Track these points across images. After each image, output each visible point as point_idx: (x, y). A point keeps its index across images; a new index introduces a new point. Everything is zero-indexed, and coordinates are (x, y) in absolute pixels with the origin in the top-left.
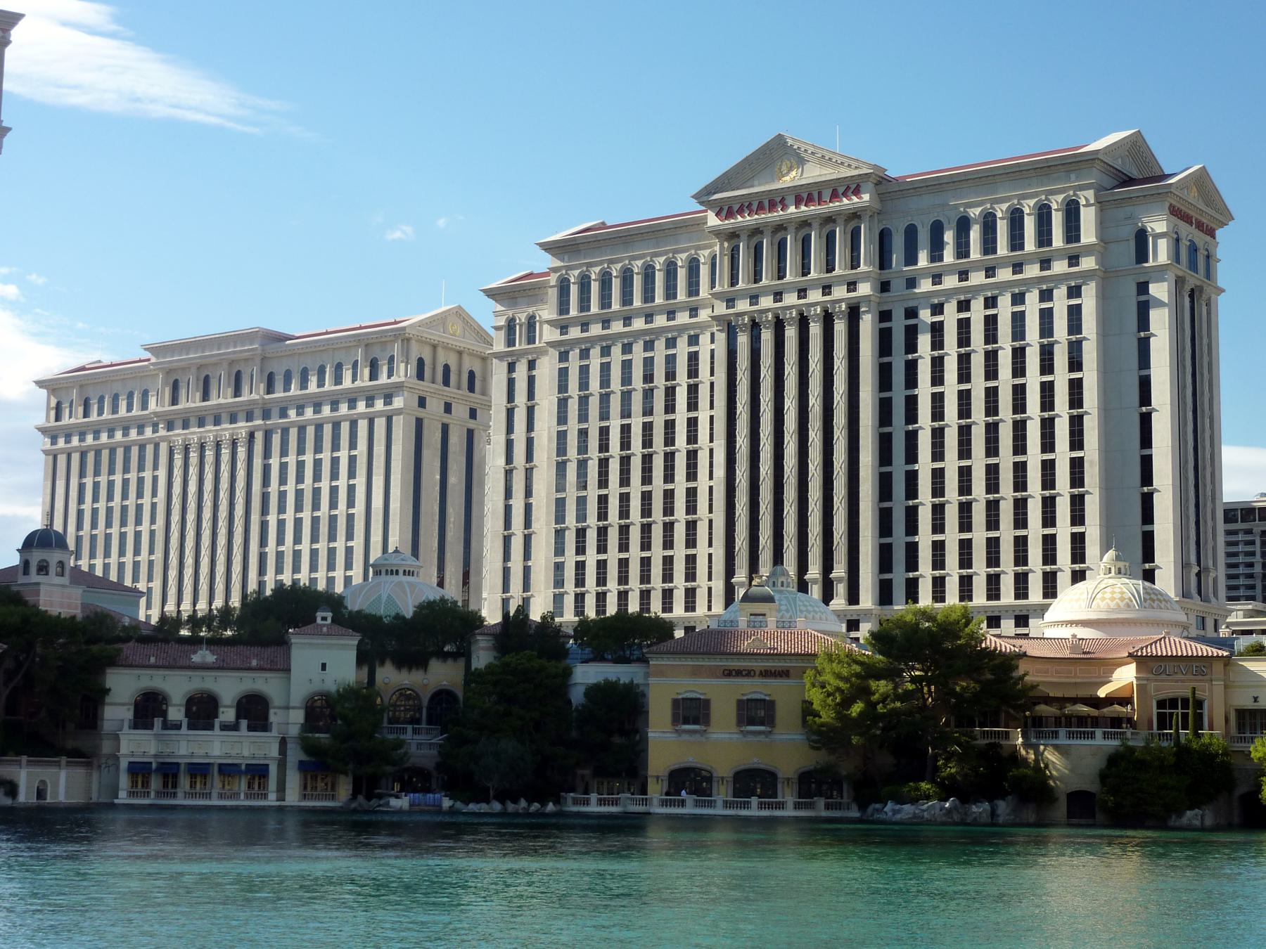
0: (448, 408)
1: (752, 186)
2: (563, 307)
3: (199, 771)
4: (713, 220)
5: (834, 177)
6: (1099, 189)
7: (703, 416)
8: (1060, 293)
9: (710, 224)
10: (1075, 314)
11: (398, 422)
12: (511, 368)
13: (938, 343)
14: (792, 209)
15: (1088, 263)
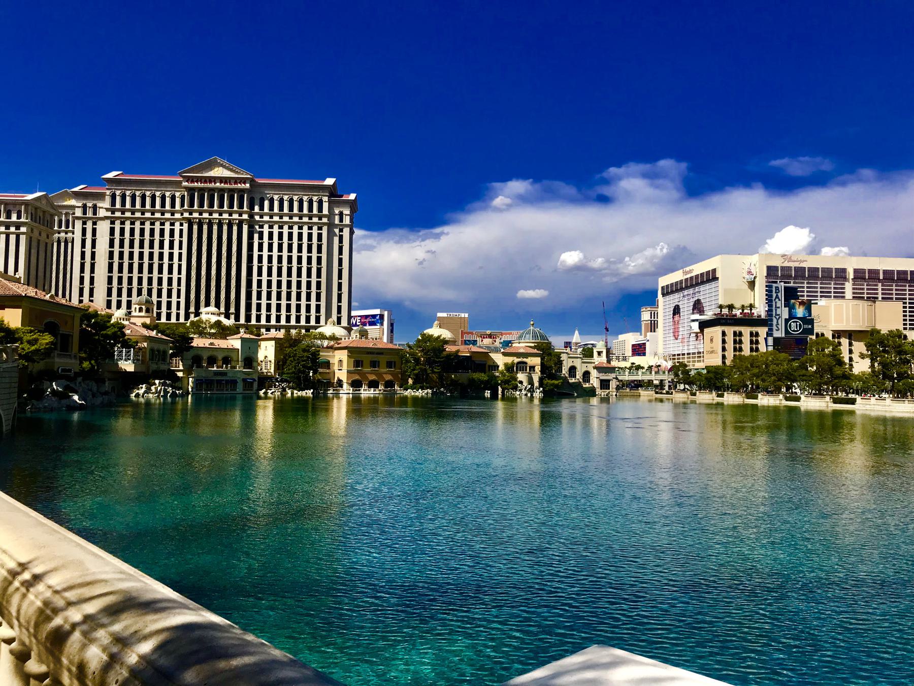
0: (40, 234)
1: (202, 173)
2: (113, 203)
7: (176, 251)
10: (320, 236)
11: (23, 239)
12: (84, 223)
14: (218, 184)
15: (325, 220)
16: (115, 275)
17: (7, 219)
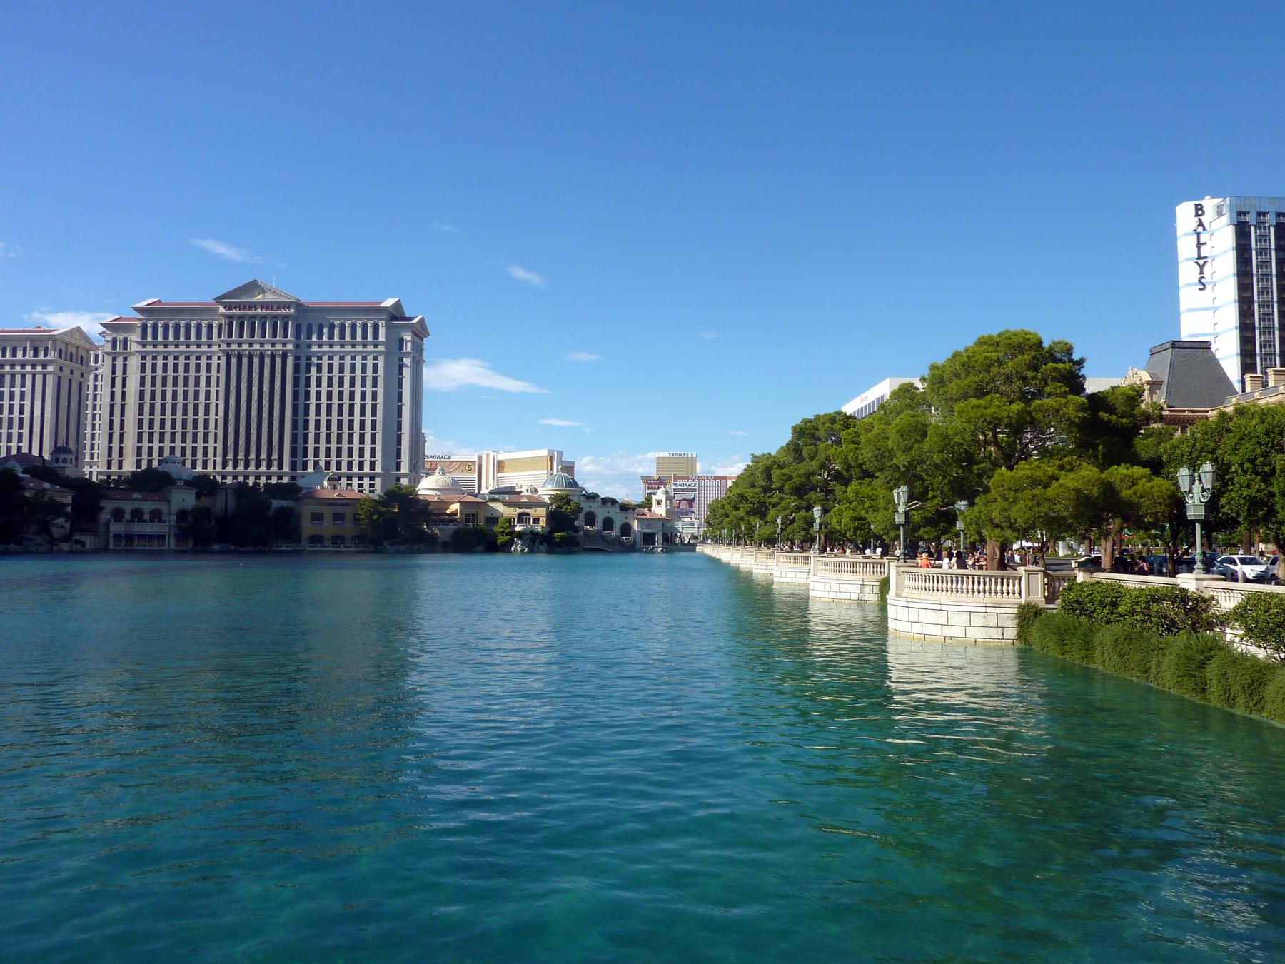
0: (72, 372)
1: (241, 299)
2: (144, 336)
3: (142, 537)
4: (222, 310)
5: (279, 301)
6: (387, 321)
7: (213, 390)
8: (370, 358)
9: (220, 311)
12: (114, 359)
13: (319, 371)
14: (259, 311)
15: (381, 348)
16: (146, 417)
17: (13, 357)
